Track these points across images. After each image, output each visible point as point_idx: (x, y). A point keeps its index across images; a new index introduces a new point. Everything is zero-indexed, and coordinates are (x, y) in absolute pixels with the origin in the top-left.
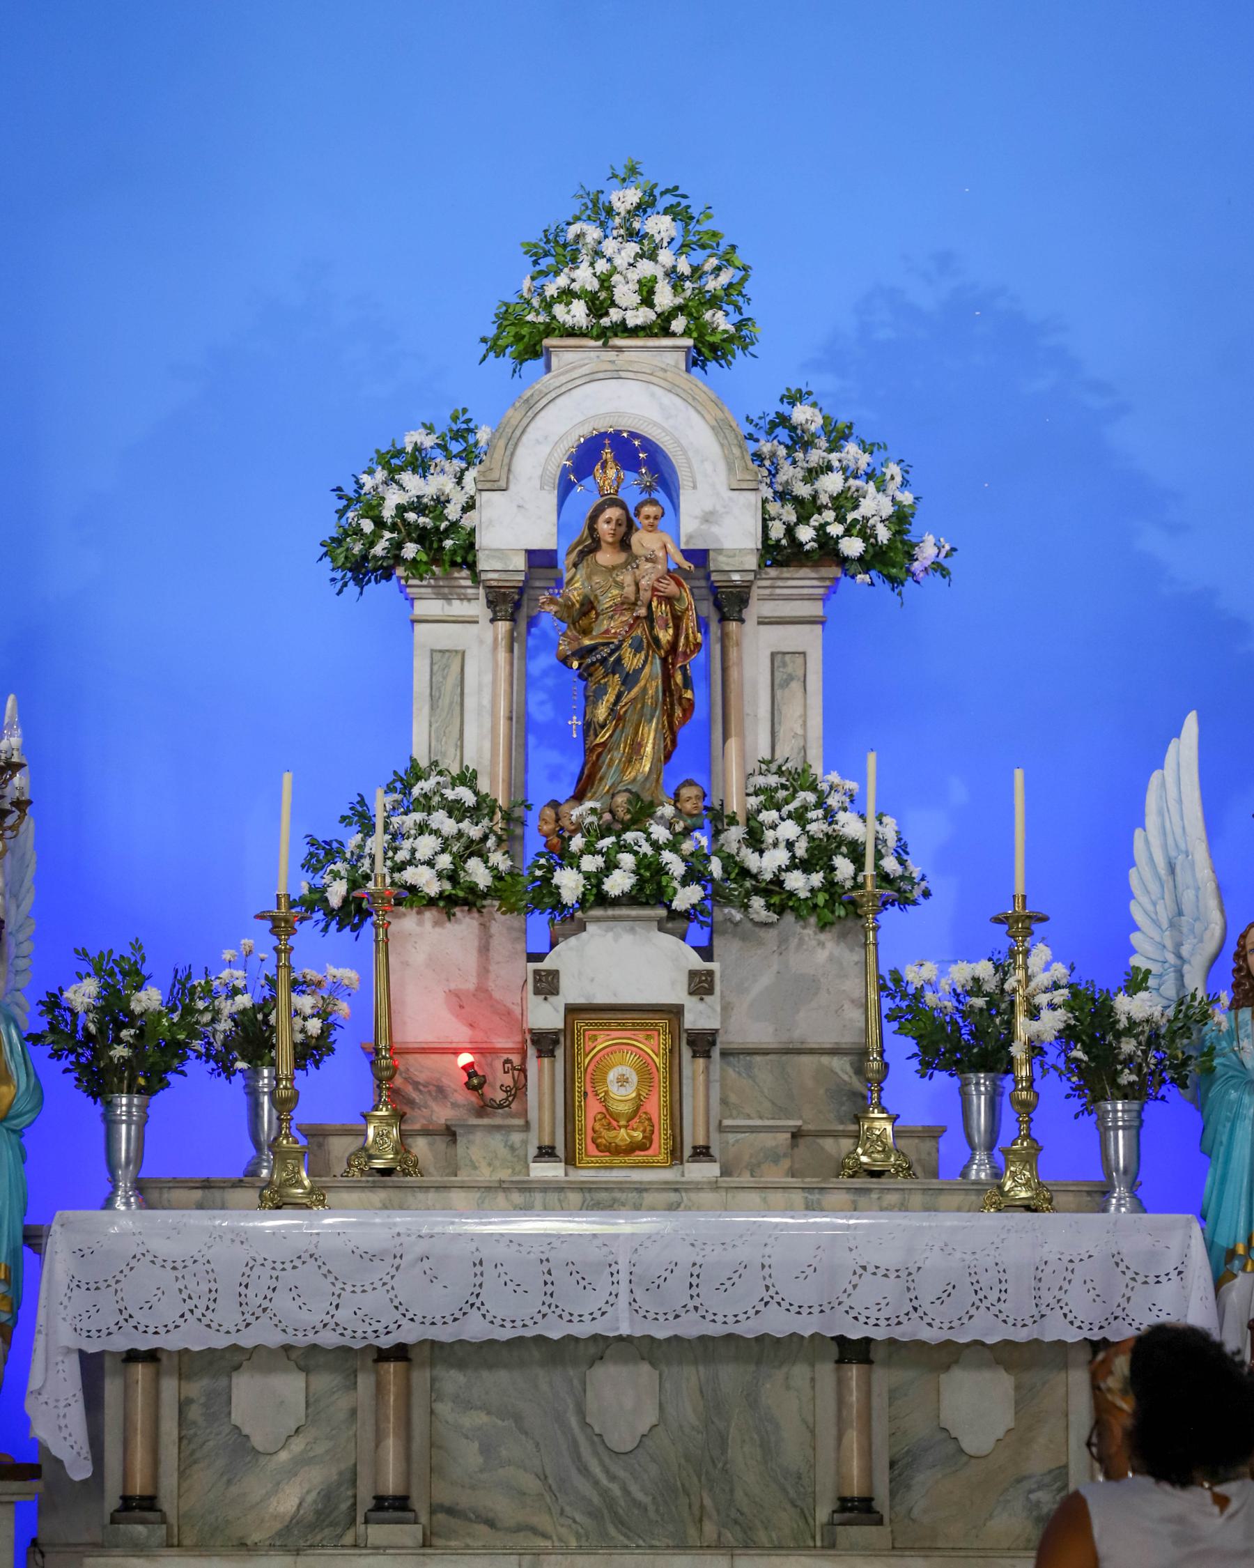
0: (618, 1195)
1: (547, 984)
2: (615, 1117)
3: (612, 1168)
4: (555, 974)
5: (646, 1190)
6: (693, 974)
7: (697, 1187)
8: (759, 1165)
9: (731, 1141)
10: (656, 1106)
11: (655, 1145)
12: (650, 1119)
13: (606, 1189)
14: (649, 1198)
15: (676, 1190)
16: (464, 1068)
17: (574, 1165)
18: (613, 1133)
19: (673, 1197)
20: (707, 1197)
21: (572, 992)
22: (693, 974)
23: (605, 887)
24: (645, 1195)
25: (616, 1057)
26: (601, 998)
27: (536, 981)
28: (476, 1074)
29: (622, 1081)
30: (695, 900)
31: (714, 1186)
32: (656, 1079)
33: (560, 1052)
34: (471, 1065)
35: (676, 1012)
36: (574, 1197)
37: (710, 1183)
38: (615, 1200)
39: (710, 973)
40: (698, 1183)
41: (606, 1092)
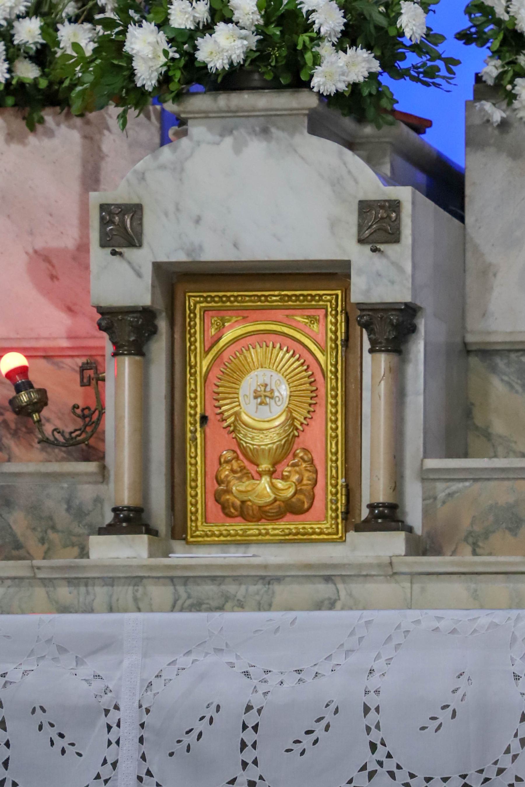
0: (231, 588)
1: (121, 227)
2: (252, 457)
3: (247, 543)
4: (136, 210)
5: (279, 580)
6: (365, 207)
7: (361, 574)
8: (486, 534)
9: (441, 496)
10: (322, 439)
11: (318, 503)
12: (312, 461)
13: (213, 579)
14: (282, 592)
15: (328, 579)
16: (10, 375)
17: (185, 539)
18: (245, 485)
19: (324, 590)
20: (380, 589)
21: (164, 242)
22: (365, 207)
23: (201, 56)
24: (277, 588)
25: (255, 355)
26: (215, 251)
27: (104, 222)
28: (28, 386)
29: (263, 395)
30: (358, 74)
31: (389, 571)
32: (322, 391)
33: (159, 348)
34: (23, 371)
35: (334, 274)
36: (160, 593)
37: (379, 566)
38: (227, 598)
39: (395, 206)
40: (360, 566)
41: (237, 415)
